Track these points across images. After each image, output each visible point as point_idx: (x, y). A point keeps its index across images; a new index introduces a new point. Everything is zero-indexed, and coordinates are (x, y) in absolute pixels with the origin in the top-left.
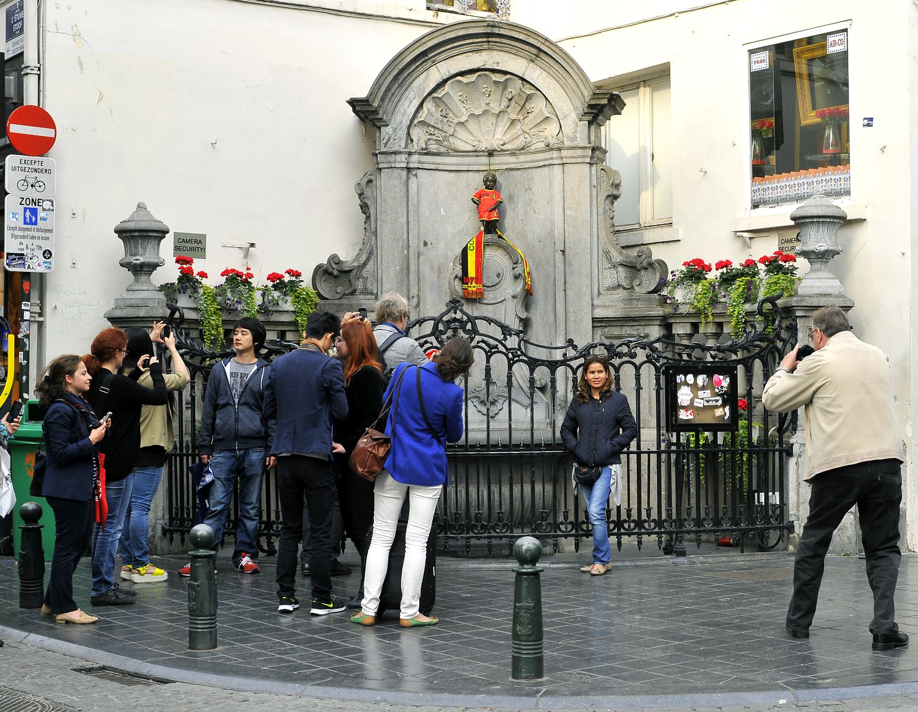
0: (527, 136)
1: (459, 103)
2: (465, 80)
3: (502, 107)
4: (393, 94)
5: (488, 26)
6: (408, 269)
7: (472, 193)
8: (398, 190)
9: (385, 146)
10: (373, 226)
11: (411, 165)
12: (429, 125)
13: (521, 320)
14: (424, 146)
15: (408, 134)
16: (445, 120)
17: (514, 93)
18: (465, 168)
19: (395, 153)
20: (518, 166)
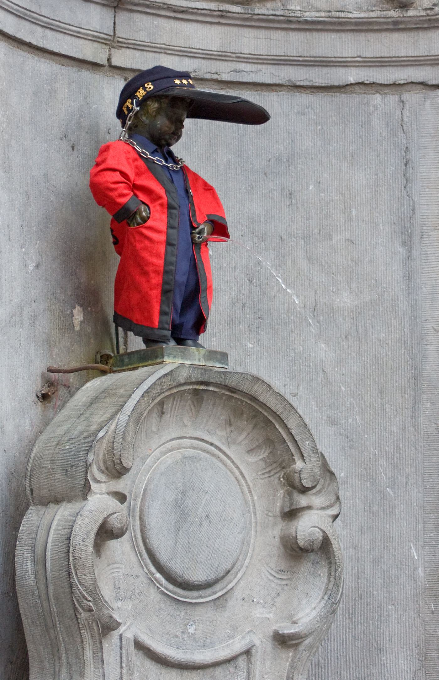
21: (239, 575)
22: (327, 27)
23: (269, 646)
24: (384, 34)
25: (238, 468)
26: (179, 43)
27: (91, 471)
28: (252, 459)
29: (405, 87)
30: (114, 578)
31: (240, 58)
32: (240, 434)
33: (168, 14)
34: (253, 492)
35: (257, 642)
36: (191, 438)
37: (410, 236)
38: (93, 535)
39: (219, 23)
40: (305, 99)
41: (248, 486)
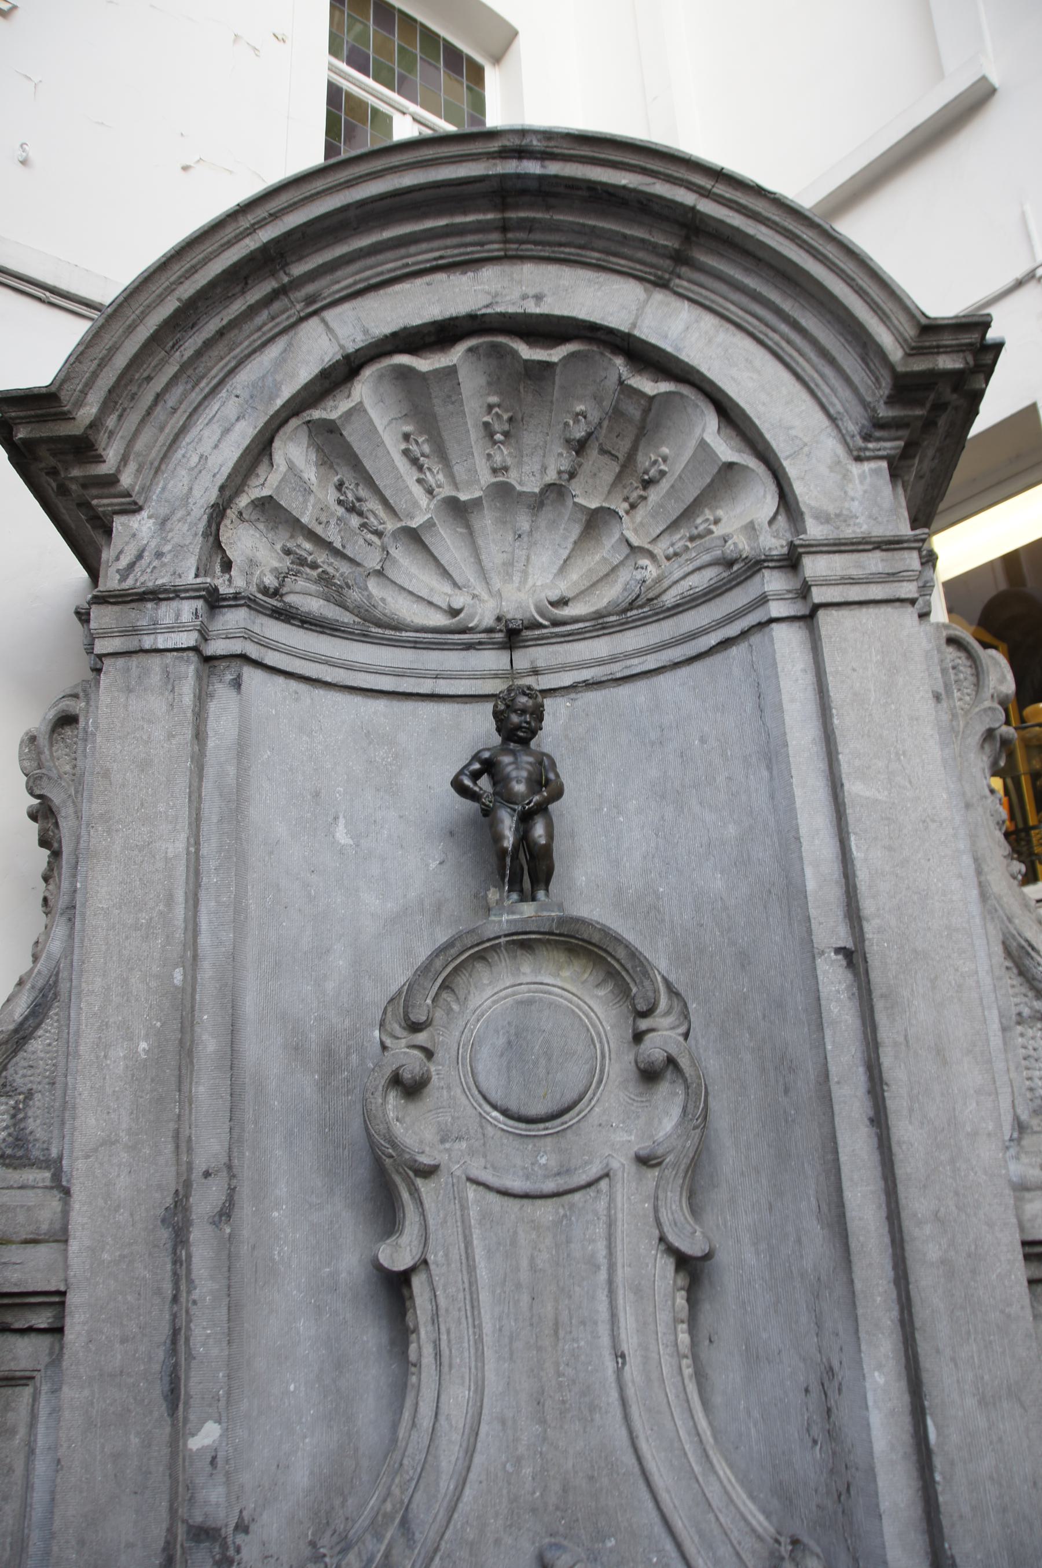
0: (645, 562)
1: (402, 464)
2: (423, 364)
3: (551, 477)
4: (158, 398)
5: (505, 154)
6: (186, 1049)
7: (455, 759)
8: (158, 733)
9: (124, 578)
10: (65, 885)
11: (217, 647)
12: (296, 525)
13: (683, 1262)
14: (270, 581)
15: (218, 545)
16: (355, 521)
17: (594, 416)
18: (426, 686)
19: (155, 595)
20: (618, 670)
21: (593, 1103)
22: (686, 607)
23: (631, 1168)
24: (726, 595)
25: (585, 1003)
26: (575, 658)
27: (386, 1030)
28: (601, 993)
29: (751, 632)
30: (439, 1122)
31: (628, 656)
32: (584, 972)
33: (559, 640)
34: (604, 1023)
35: (615, 1165)
36: (527, 984)
37: (770, 760)
38: (381, 1088)
39: (604, 635)
40: (684, 672)
41: (598, 1018)
